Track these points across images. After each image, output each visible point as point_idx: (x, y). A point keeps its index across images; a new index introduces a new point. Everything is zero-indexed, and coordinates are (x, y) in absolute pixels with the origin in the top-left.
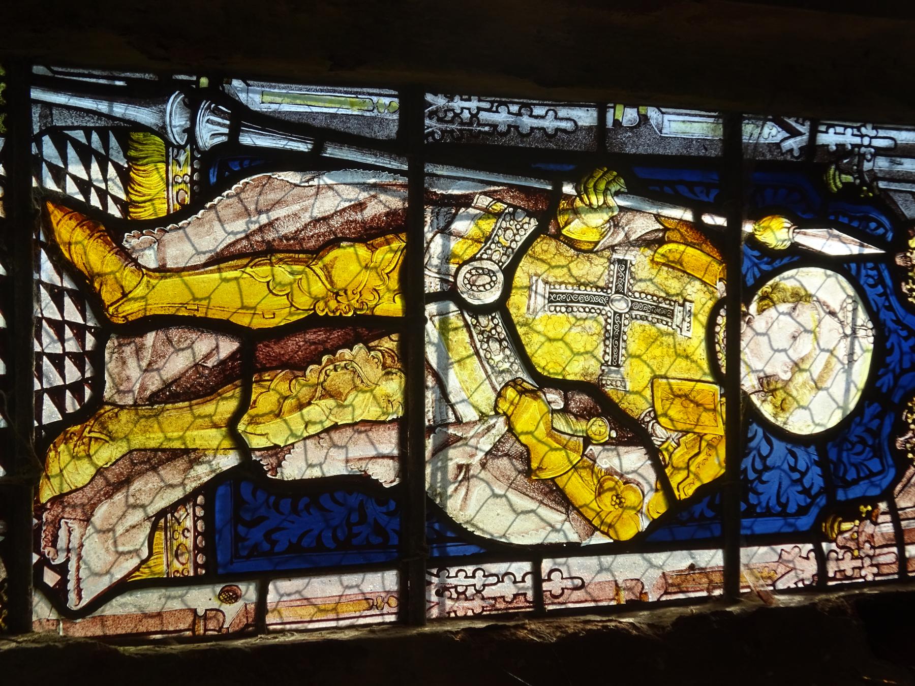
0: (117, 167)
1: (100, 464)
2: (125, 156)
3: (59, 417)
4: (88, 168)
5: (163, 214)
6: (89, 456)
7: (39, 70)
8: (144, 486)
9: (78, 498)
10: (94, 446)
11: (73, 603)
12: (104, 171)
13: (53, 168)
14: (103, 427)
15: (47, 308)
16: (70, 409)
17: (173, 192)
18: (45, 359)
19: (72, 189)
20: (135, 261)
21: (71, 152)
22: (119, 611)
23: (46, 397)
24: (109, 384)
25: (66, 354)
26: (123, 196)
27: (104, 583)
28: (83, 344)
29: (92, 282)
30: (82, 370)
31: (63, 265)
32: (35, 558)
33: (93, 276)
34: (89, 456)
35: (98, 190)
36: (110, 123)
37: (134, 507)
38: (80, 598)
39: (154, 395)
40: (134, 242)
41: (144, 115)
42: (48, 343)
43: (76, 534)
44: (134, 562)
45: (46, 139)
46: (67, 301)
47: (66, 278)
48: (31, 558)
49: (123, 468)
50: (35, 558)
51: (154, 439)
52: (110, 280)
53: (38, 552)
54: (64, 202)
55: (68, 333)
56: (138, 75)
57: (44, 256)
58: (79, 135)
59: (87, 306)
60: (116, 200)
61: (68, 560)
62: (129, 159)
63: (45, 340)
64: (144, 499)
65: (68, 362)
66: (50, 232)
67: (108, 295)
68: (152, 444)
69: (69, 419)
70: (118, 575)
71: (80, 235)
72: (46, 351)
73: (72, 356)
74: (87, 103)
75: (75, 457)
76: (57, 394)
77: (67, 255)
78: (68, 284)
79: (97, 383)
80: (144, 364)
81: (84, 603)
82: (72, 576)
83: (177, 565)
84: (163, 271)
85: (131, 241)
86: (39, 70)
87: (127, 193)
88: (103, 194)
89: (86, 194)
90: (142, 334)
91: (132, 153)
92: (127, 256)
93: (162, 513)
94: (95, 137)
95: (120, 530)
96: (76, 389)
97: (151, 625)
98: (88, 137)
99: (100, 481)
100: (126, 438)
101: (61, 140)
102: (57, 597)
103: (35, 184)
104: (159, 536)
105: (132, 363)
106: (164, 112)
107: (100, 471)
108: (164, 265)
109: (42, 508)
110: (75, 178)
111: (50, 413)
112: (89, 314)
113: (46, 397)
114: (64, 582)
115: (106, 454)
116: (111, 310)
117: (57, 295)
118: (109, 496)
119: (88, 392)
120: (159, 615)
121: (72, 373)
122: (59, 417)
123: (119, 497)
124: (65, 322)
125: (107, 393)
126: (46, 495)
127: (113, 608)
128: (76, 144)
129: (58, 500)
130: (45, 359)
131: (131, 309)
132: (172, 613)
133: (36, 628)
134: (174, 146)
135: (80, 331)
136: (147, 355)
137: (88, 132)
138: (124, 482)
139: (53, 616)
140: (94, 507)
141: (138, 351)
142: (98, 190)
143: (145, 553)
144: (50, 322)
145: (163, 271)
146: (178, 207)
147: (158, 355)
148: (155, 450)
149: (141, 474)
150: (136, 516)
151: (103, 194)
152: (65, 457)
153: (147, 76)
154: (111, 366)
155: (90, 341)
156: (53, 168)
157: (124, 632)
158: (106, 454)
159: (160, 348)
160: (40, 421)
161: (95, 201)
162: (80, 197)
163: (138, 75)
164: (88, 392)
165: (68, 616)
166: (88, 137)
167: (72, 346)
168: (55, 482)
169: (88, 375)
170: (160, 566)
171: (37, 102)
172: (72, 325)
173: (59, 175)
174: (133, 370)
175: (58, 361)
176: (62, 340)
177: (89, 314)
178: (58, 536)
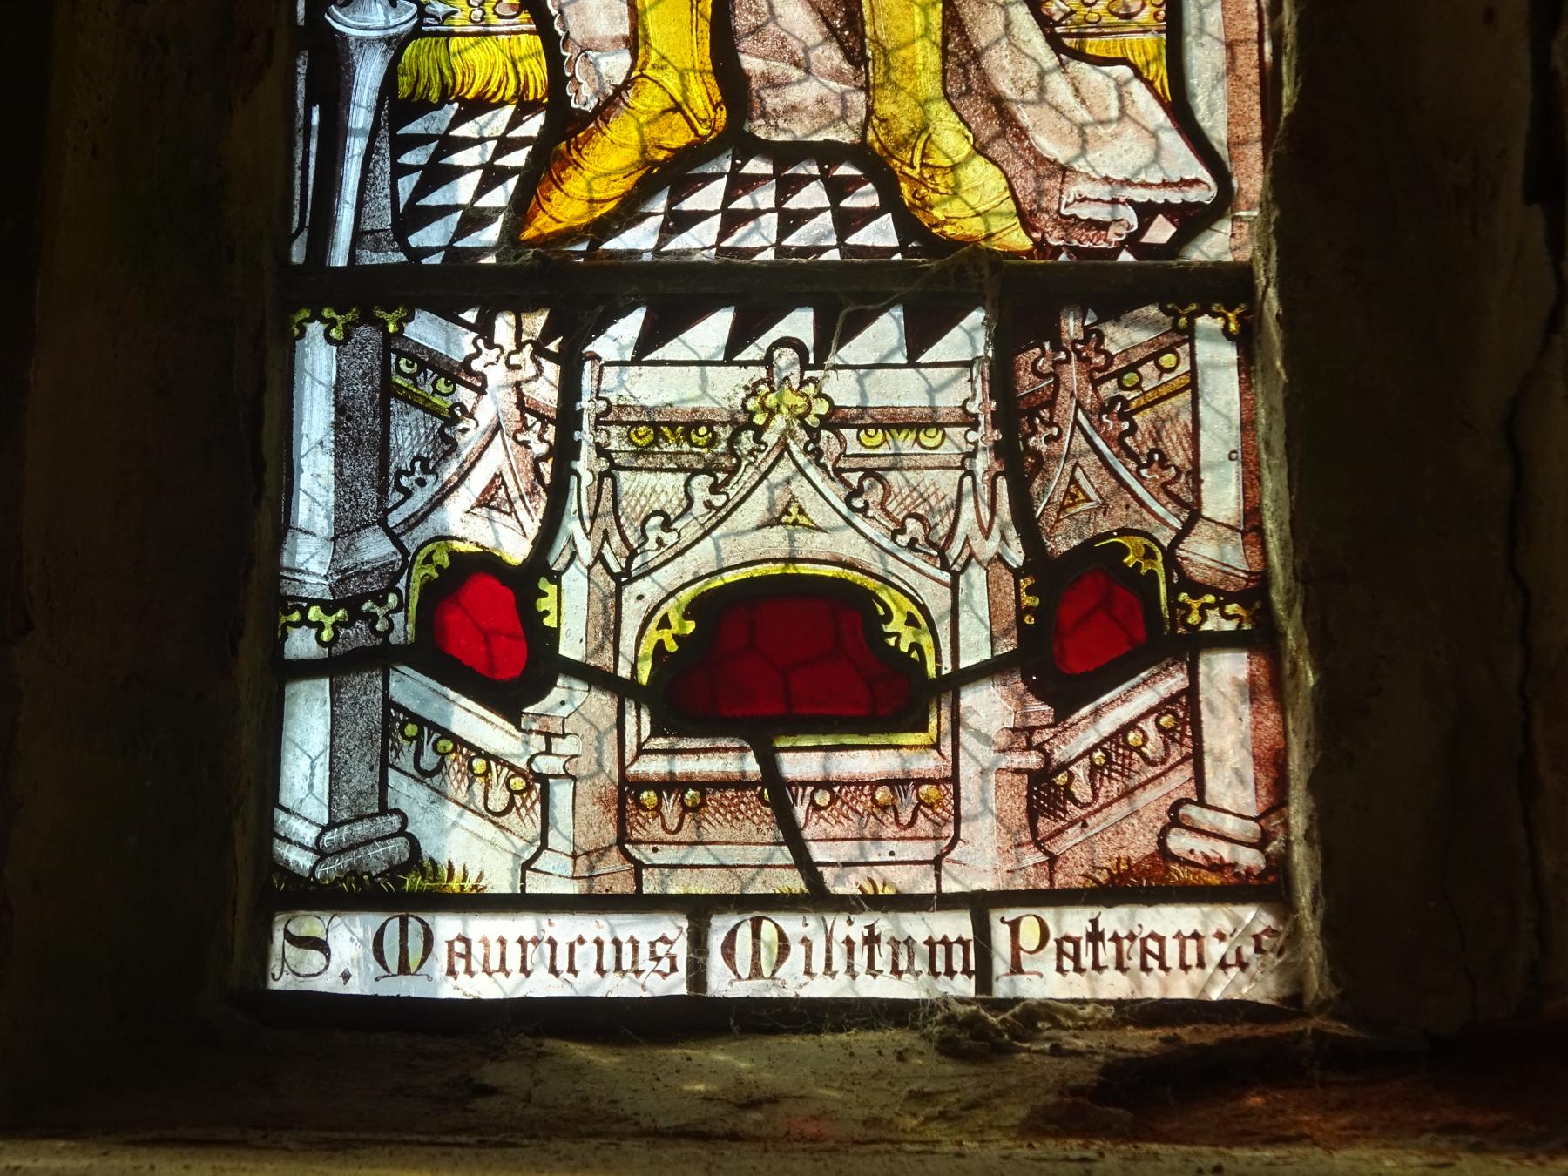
0: (458, 120)
1: (966, 148)
2: (439, 106)
3: (887, 219)
4: (460, 171)
5: (537, 42)
6: (954, 168)
7: (298, 254)
8: (1006, 73)
9: (1026, 186)
10: (937, 159)
11: (1204, 194)
12: (466, 143)
13: (464, 229)
14: (904, 143)
15: (700, 239)
16: (873, 200)
17: (498, 24)
18: (787, 242)
19: (498, 197)
20: (618, 90)
21: (435, 199)
22: (1222, 115)
23: (853, 240)
24: (830, 135)
25: (778, 207)
26: (509, 111)
27: (1174, 142)
28: (765, 178)
29: (655, 163)
30: (807, 179)
31: (628, 212)
32: (1126, 257)
33: (646, 162)
34: (954, 168)
35: (498, 153)
36: (384, 132)
37: (1042, 90)
38: (1197, 182)
39: (849, 56)
40: (586, 92)
41: (368, 75)
42: (760, 238)
43: (1086, 189)
44: (1138, 90)
45: (415, 240)
46: (688, 205)
47: (649, 208)
48: (1126, 265)
49: (975, 110)
50: (1126, 257)
51: (926, 56)
52: (652, 132)
53: (1117, 252)
54: (521, 208)
55: (743, 203)
56: (301, 86)
57: (612, 245)
58: (407, 185)
59: (697, 171)
60: (515, 122)
61: (1131, 202)
62: (444, 100)
63: (754, 242)
64: (1029, 73)
65: (793, 204)
66: (571, 235)
67: (679, 137)
68: (934, 59)
69: (891, 201)
70: (1159, 116)
71: (575, 184)
72: (774, 240)
73: (782, 196)
74: (352, 172)
75: (955, 192)
76: (847, 222)
77: (611, 205)
78: (660, 204)
79: (828, 154)
80: (796, 74)
81: (1204, 174)
82: (1158, 197)
83: (1145, 17)
84: (634, 42)
85: (584, 97)
86: (298, 254)
87: (502, 103)
88: (506, 145)
89: (505, 173)
90: (743, 78)
91: (434, 95)
92: (610, 104)
93: (1055, 42)
94: (408, 158)
95: (1081, 115)
96: (838, 189)
97: (1248, 61)
98: (409, 169)
99: (997, 149)
100: (923, 104)
101: (413, 217)
102: (1193, 221)
103: (491, 260)
104: (1093, 47)
105: (794, 95)
106: (361, 41)
107: (980, 150)
108: (626, 40)
109: (1041, 245)
110: (480, 192)
111: (880, 234)
112: (710, 169)
113: (853, 240)
114: (1168, 209)
115: (950, 139)
116: (703, 131)
117: (678, 222)
118: (1022, 134)
119: (844, 170)
120: (1230, 46)
121: (812, 196)
122: (887, 219)
123: (1025, 116)
124: (724, 209)
125: (846, 136)
126: (1019, 240)
127: (1216, 126)
128: (421, 190)
129: (1027, 221)
130: (787, 242)
131: (702, 96)
132: (1227, 24)
133: (1244, 255)
134: (420, 23)
135: (740, 184)
136: (780, 68)
137: (399, 171)
138: (1000, 107)
139: (1225, 226)
140: (1041, 160)
141: (773, 84)
142: (498, 153)
143: (1123, 71)
144: (724, 233)
145: (634, 42)
146: (525, 16)
147: (781, 50)
148: (945, 55)
149: (985, 79)
150: (1059, 87)
151: (506, 145)
152: (955, 208)
153: (302, 70)
154: (799, 130)
155: (757, 166)
156: (464, 229)
157: (1258, 107)
158: (950, 139)
159: (769, 45)
160: (893, 251)
161: (517, 158)
162: (512, 182)
163: (301, 86)
164: (844, 170)
165: (1226, 200)
166: (409, 169)
167: (765, 197)
168: (996, 224)
169: (814, 170)
170: (1146, 45)
171: (352, 256)
172: (730, 196)
173: (474, 219)
174: (807, 92)
175: (791, 221)
176: (756, 214)
177: (710, 169)
178: (1089, 220)
